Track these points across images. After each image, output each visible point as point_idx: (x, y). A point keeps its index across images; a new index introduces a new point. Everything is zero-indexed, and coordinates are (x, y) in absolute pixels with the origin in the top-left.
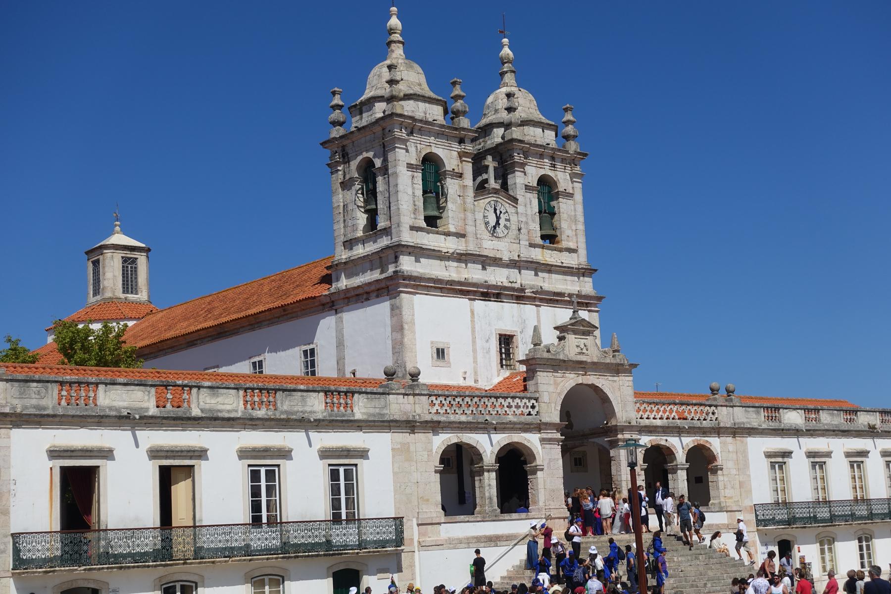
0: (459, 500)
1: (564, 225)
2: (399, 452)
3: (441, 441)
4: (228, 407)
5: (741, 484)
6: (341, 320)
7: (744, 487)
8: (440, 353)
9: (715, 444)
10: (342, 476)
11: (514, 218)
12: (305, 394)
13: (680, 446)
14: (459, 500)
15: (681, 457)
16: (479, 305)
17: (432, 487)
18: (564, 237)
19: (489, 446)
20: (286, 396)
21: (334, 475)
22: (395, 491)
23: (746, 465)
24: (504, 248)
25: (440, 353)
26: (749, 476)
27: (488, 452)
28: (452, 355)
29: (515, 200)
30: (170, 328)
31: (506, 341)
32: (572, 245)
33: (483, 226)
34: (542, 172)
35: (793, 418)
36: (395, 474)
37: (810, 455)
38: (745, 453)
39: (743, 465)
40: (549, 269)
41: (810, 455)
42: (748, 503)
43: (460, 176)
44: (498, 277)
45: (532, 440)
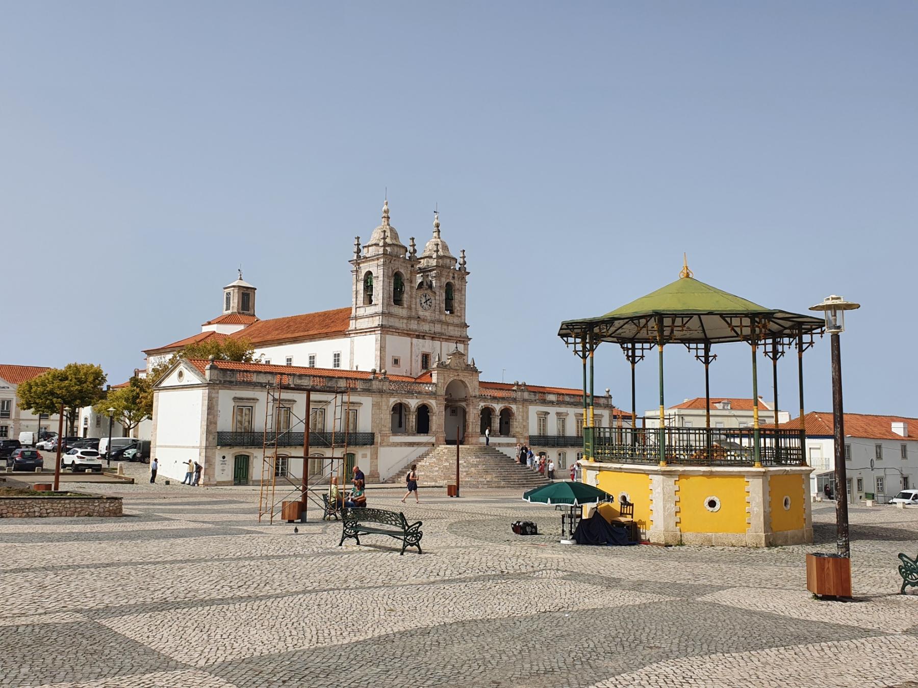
0: (399, 426)
1: (456, 305)
3: (393, 401)
6: (352, 342)
7: (526, 427)
8: (396, 362)
9: (514, 407)
11: (433, 302)
13: (498, 407)
14: (399, 426)
15: (498, 412)
16: (415, 340)
19: (413, 403)
23: (527, 418)
24: (427, 314)
25: (396, 362)
28: (401, 362)
30: (268, 333)
31: (426, 358)
37: (558, 414)
38: (527, 412)
40: (448, 324)
41: (558, 414)
42: (526, 435)
44: (426, 327)
45: (432, 403)
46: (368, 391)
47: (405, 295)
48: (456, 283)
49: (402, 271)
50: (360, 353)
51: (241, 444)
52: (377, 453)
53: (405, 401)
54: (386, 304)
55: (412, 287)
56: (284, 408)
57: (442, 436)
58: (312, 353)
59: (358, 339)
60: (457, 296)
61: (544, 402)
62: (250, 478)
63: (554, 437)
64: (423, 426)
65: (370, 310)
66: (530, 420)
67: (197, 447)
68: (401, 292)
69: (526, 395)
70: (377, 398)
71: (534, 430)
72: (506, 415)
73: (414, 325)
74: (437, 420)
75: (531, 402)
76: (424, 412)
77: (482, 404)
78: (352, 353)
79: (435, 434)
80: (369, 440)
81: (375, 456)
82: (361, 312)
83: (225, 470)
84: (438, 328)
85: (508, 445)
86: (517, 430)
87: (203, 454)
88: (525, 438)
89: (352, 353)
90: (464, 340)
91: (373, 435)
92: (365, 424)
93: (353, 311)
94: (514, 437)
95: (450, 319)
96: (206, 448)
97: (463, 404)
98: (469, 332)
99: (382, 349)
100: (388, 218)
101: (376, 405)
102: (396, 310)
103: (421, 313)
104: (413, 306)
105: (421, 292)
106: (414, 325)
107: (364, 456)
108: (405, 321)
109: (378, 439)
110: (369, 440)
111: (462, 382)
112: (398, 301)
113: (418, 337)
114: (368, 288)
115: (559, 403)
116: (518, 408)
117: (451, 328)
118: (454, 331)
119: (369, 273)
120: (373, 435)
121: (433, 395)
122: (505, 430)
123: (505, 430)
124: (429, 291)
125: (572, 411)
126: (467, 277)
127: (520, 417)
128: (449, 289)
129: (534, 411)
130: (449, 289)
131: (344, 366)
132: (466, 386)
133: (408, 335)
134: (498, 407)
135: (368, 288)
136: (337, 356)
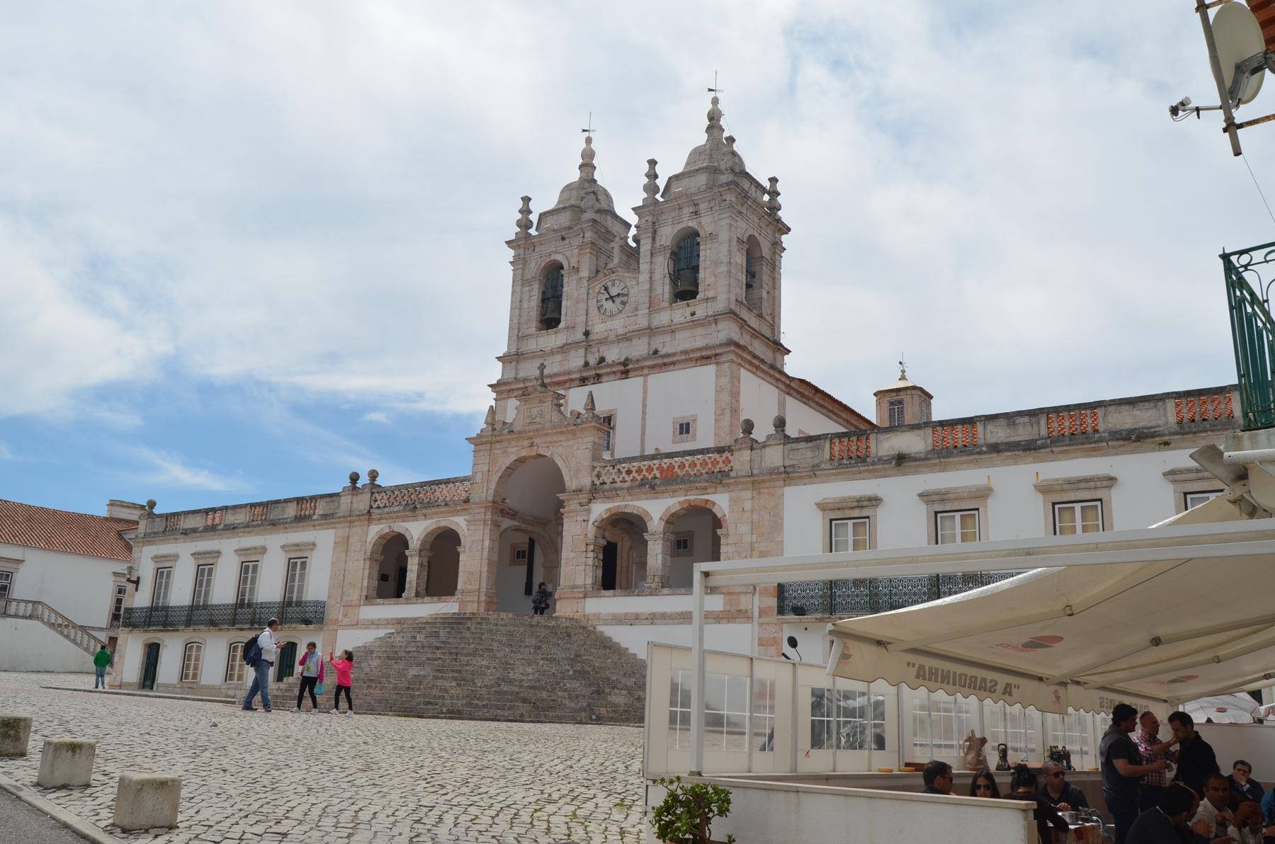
2: (343, 545)
3: (375, 531)
9: (721, 502)
10: (296, 567)
11: (632, 292)
15: (656, 523)
17: (361, 573)
26: (781, 542)
27: (415, 538)
32: (710, 294)
46: (329, 519)
53: (400, 527)
70: (342, 530)
77: (600, 510)
84: (639, 348)
92: (316, 587)
95: (680, 313)
112: (550, 320)
116: (733, 501)
117: (680, 335)
127: (744, 528)
134: (656, 510)
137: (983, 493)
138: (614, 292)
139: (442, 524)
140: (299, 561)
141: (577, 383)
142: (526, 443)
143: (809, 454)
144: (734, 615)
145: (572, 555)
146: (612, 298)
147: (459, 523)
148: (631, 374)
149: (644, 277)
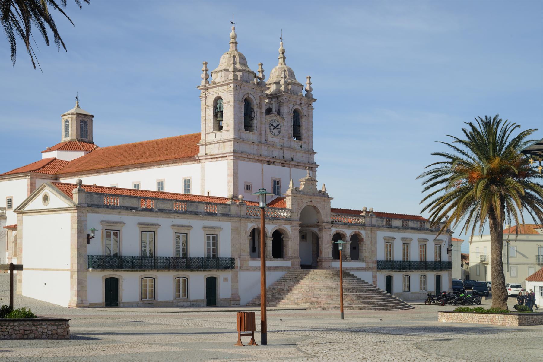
3: (250, 226)
4: (168, 209)
5: (372, 251)
6: (203, 168)
7: (373, 252)
8: (248, 187)
9: (363, 233)
11: (282, 128)
12: (198, 204)
13: (348, 232)
15: (348, 238)
16: (266, 166)
18: (303, 137)
19: (270, 228)
20: (191, 205)
21: (208, 238)
22: (232, 246)
23: (375, 243)
24: (276, 140)
25: (248, 187)
29: (283, 118)
33: (269, 131)
34: (295, 107)
35: (397, 223)
36: (232, 239)
37: (403, 239)
39: (374, 243)
41: (403, 239)
42: (374, 259)
43: (261, 108)
47: (255, 121)
48: (304, 110)
49: (251, 97)
50: (212, 177)
51: (113, 268)
52: (237, 277)
54: (237, 130)
55: (262, 113)
56: (150, 230)
57: (298, 261)
58: (160, 178)
59: (209, 165)
60: (304, 122)
61: (390, 226)
62: (120, 299)
63: (399, 262)
64: (278, 251)
65: (220, 135)
66: (377, 245)
67: (67, 270)
68: (252, 118)
69: (374, 221)
71: (381, 255)
72: (356, 239)
73: (264, 151)
74: (293, 244)
75: (379, 227)
76: (278, 236)
78: (203, 179)
79: (291, 258)
80: (229, 264)
81: (235, 280)
82: (211, 138)
83: (98, 293)
85: (358, 269)
86: (367, 255)
87: (75, 276)
88: (373, 262)
89: (203, 179)
90: (313, 166)
91: (232, 260)
92: (225, 250)
93: (203, 137)
94: (363, 261)
96: (79, 270)
97: (316, 230)
98: (317, 159)
99: (235, 174)
100: (236, 43)
101: (235, 231)
102: (247, 135)
103: (271, 139)
104: (263, 132)
105: (270, 118)
106: (264, 151)
107: (226, 280)
108: (256, 147)
109: (238, 263)
110: (229, 264)
111: (314, 207)
113: (268, 162)
114: (218, 114)
115: (405, 228)
116: (366, 234)
118: (300, 157)
119: (218, 99)
120: (232, 260)
121: (288, 220)
122: (355, 254)
123: (355, 254)
124: (278, 118)
125: (415, 237)
126: (314, 104)
127: (369, 243)
128: (296, 116)
129: (381, 235)
130: (296, 116)
131: (195, 191)
132: (318, 212)
133: (260, 161)
135: (218, 114)
136: (187, 183)
137: (411, 239)
138: (275, 125)
139: (281, 228)
140: (211, 236)
141: (265, 162)
142: (309, 200)
143: (381, 222)
144: (367, 269)
145: (327, 246)
146: (275, 128)
147: (287, 228)
148: (285, 165)
149: (286, 124)
